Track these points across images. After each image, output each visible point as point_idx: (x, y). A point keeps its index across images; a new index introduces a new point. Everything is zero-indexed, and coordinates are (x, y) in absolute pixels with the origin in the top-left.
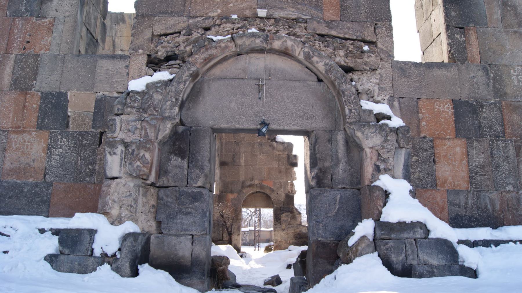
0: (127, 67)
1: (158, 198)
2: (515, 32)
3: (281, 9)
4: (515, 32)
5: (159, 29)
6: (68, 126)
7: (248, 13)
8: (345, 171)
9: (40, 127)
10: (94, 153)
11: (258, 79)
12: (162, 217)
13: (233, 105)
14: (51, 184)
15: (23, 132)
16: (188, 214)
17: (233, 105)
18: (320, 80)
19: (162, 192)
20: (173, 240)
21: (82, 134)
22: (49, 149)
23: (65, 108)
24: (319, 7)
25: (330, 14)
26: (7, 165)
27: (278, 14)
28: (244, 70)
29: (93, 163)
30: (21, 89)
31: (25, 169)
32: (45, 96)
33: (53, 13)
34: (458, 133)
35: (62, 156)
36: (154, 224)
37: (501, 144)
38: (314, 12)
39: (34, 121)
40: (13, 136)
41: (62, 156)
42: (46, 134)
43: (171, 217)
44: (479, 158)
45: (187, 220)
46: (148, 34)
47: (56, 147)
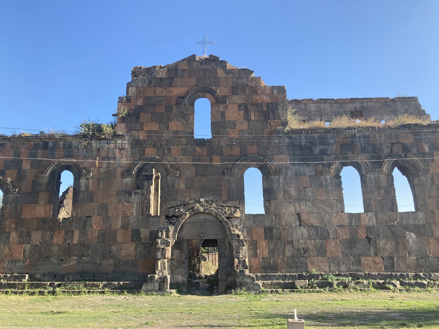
0: (159, 220)
1: (171, 263)
2: (288, 201)
3: (208, 197)
4: (288, 201)
5: (169, 206)
6: (141, 240)
7: (197, 199)
8: (228, 252)
9: (132, 241)
10: (150, 249)
11: (201, 222)
12: (173, 269)
13: (193, 231)
14: (137, 260)
15: (127, 243)
16: (180, 268)
17: (193, 231)
18: (221, 222)
19: (172, 262)
20: (176, 276)
21: (146, 243)
22: (136, 249)
23: (140, 234)
24: (220, 196)
25: (224, 198)
26: (123, 254)
27: (207, 199)
28: (197, 219)
29: (150, 253)
30: (124, 229)
31: (128, 255)
32: (133, 231)
33: (133, 201)
34: (265, 238)
35: (140, 251)
36: (170, 271)
37: (279, 241)
38: (219, 198)
39: (130, 239)
40: (123, 245)
41: (140, 251)
42: (135, 244)
43: (176, 269)
44: (271, 247)
45: (180, 270)
46: (165, 208)
47: (138, 248)
